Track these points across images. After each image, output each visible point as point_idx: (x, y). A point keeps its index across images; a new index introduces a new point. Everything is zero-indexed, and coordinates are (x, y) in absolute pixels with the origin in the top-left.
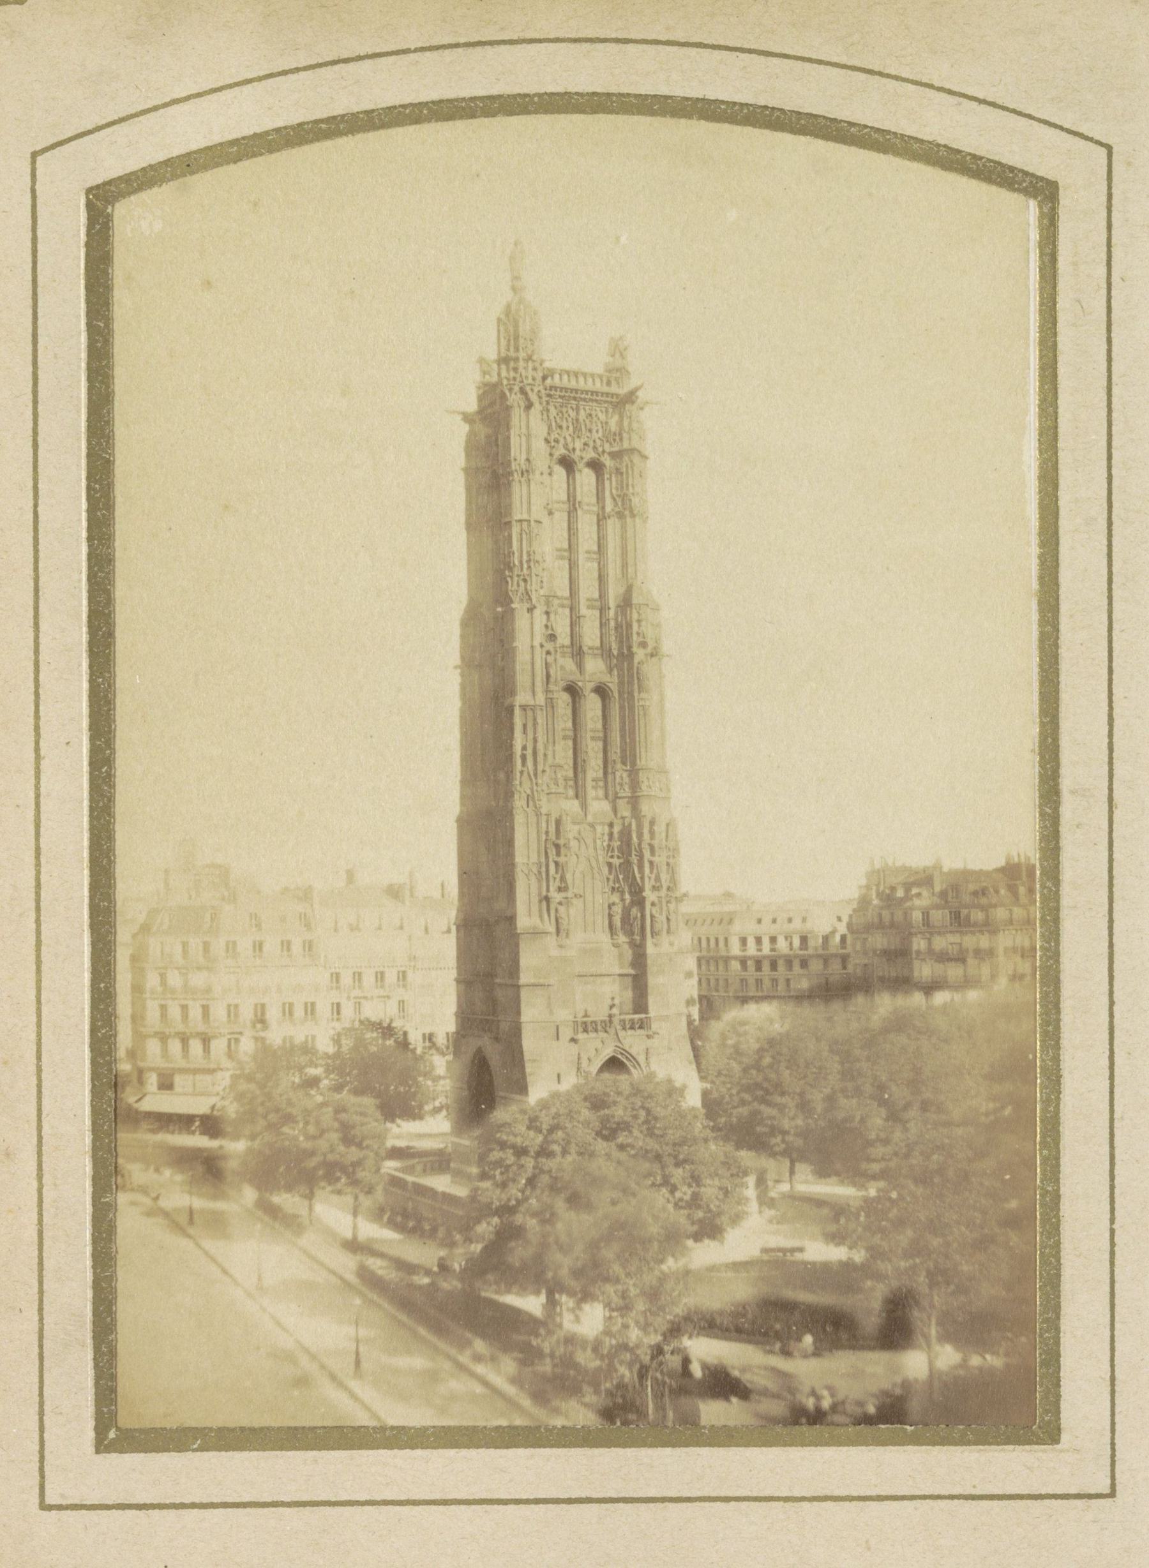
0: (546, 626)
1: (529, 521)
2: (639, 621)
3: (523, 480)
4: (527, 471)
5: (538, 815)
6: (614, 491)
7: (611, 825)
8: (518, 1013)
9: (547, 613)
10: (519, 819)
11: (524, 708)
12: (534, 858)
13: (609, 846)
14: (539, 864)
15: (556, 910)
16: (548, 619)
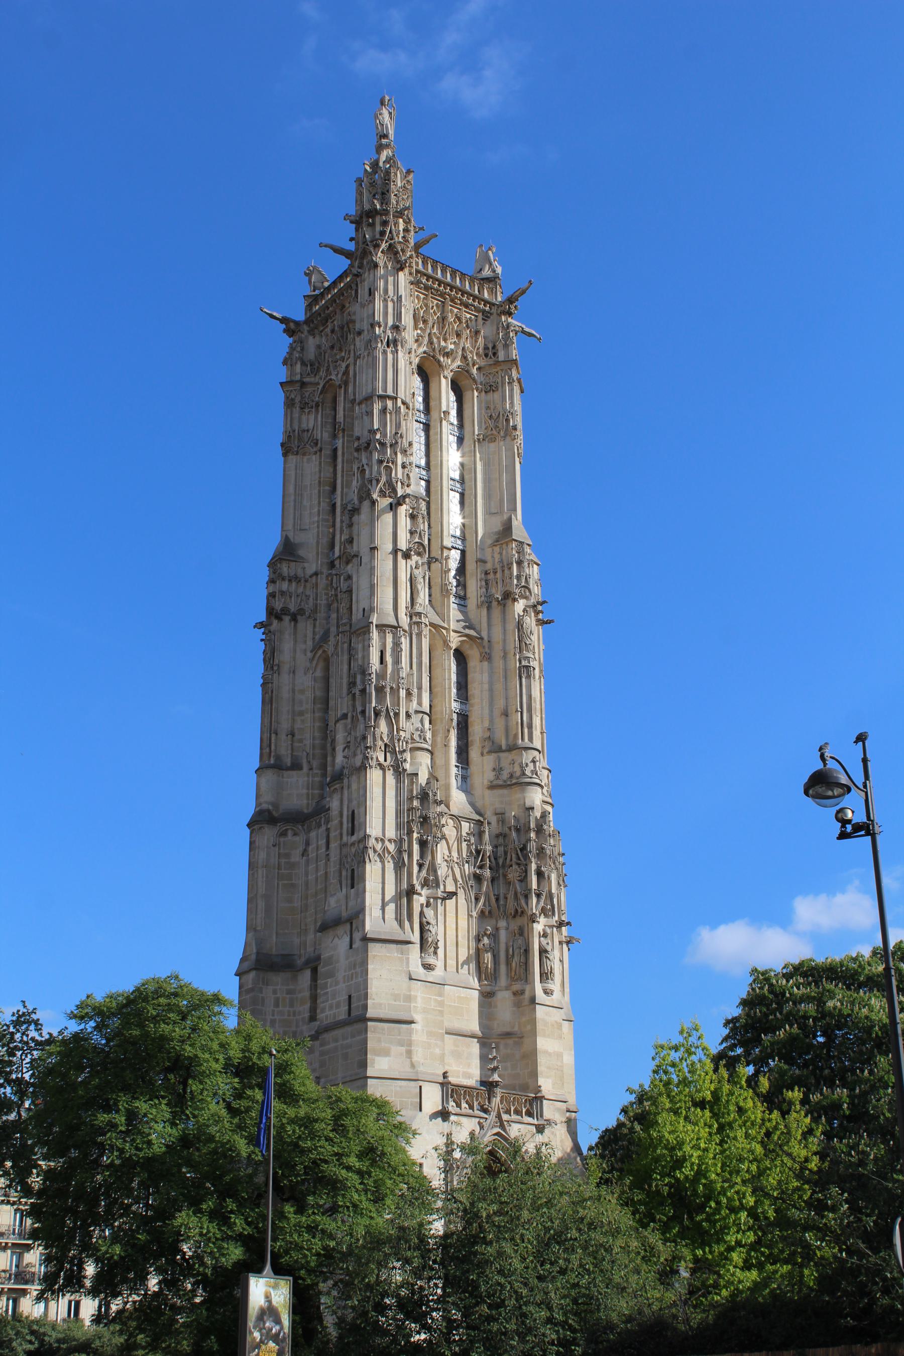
0: (412, 533)
1: (394, 399)
2: (520, 563)
3: (389, 350)
4: (395, 342)
5: (399, 771)
6: (483, 412)
7: (479, 823)
8: (364, 1064)
9: (413, 517)
10: (374, 776)
11: (381, 627)
12: (391, 833)
13: (478, 852)
14: (399, 842)
15: (422, 914)
16: (413, 524)
